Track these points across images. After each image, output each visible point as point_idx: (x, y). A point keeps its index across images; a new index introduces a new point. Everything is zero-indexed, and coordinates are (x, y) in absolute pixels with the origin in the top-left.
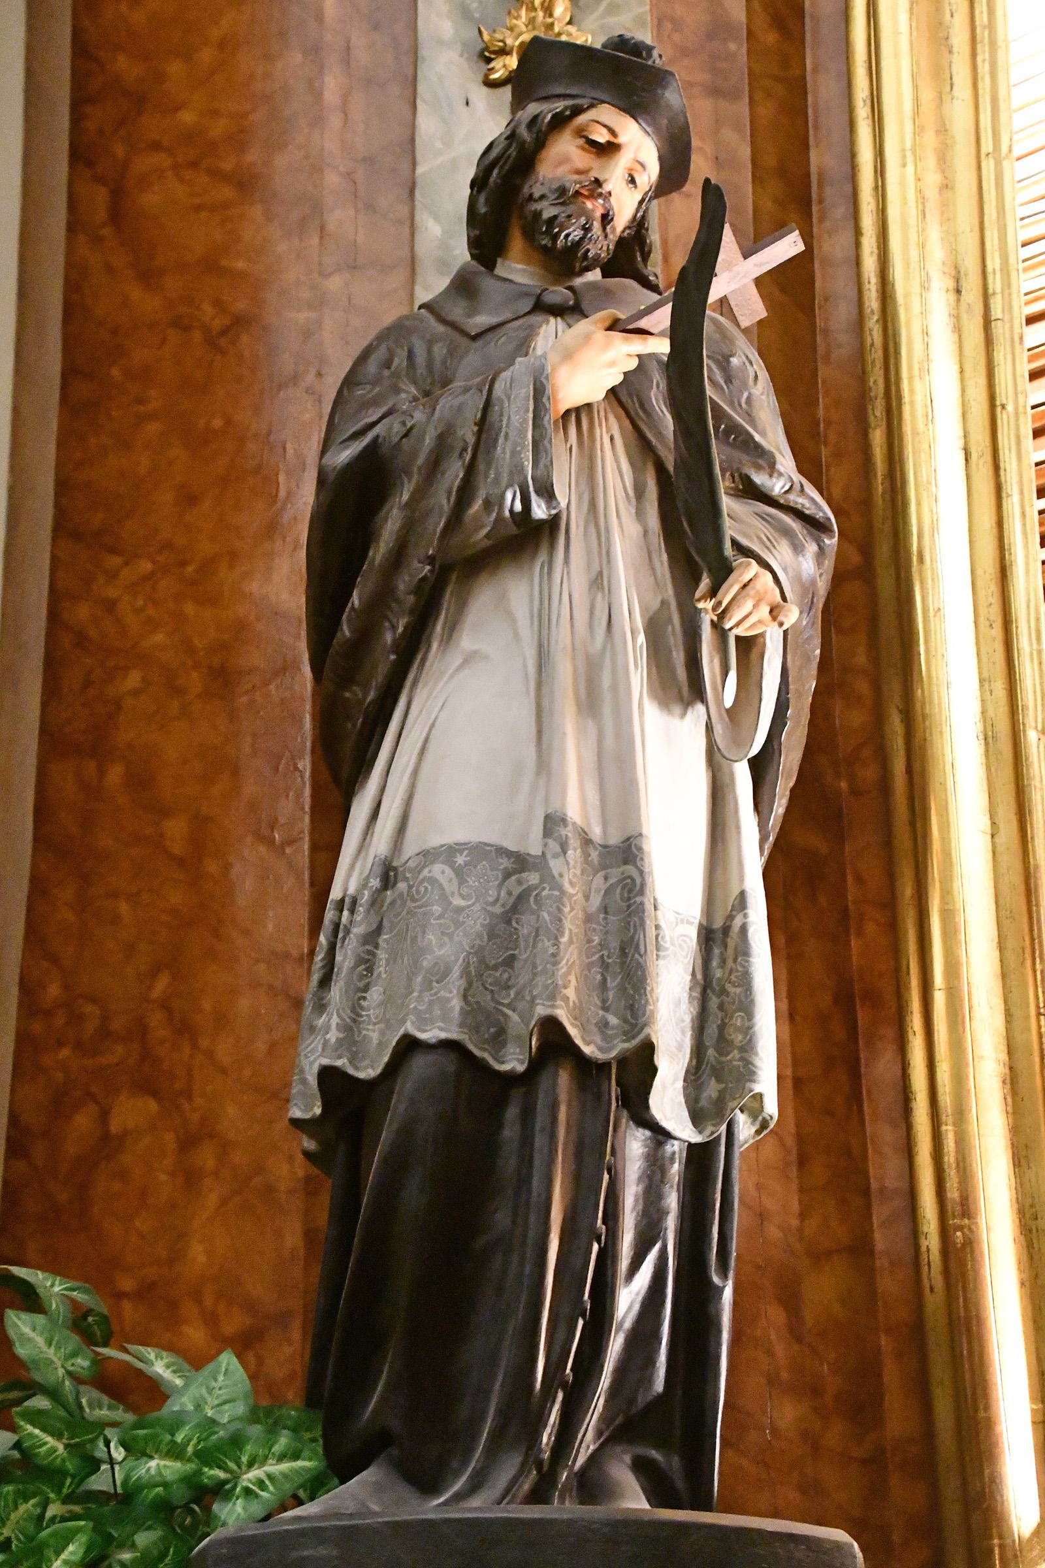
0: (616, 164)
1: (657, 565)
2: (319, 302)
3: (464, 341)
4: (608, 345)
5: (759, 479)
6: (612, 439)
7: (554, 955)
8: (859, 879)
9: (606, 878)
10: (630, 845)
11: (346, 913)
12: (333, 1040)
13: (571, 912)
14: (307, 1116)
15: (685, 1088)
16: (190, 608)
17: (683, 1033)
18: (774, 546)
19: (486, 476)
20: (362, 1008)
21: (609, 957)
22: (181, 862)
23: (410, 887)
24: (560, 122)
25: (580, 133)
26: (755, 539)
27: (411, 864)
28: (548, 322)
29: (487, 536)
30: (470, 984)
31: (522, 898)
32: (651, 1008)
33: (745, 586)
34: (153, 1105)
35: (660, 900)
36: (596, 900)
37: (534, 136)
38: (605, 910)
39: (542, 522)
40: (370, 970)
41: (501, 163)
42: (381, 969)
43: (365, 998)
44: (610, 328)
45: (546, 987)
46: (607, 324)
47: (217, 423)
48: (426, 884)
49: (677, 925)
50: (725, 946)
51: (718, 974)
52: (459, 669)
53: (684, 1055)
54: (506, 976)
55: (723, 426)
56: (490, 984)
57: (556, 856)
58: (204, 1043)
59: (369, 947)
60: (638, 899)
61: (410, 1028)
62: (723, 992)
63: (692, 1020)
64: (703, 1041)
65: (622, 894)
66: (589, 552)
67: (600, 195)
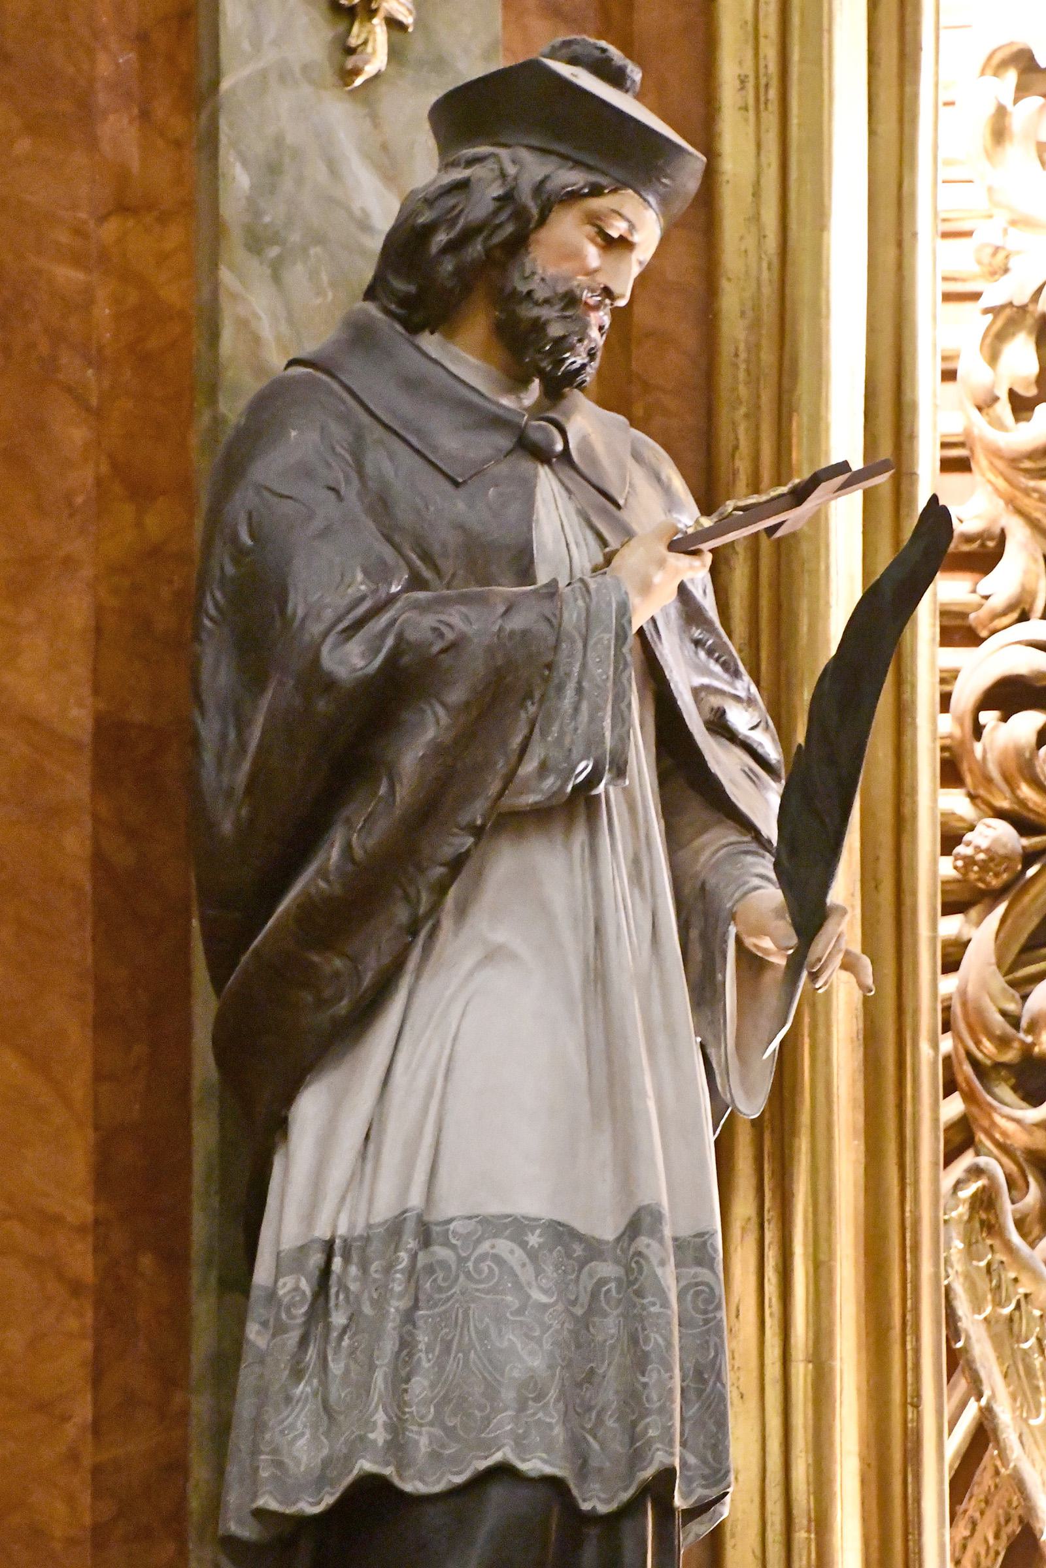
24: (573, 197)
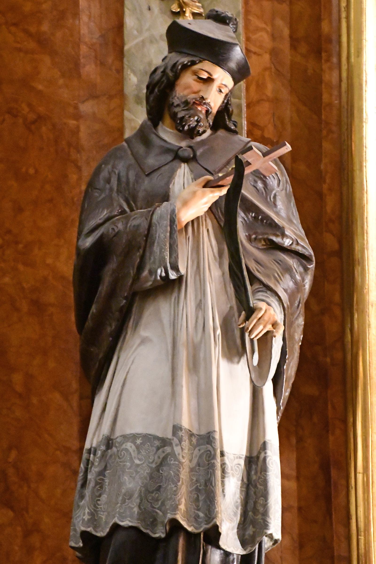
0: (212, 90)
1: (229, 289)
2: (78, 116)
3: (143, 176)
4: (204, 195)
5: (277, 240)
6: (208, 230)
7: (175, 491)
8: (334, 408)
9: (199, 450)
10: (209, 436)
11: (92, 455)
12: (86, 519)
13: (183, 470)
14: (77, 546)
15: (238, 532)
16: (21, 267)
17: (237, 508)
18: (281, 280)
19: (150, 259)
20: (98, 505)
21: (200, 486)
22: (20, 396)
23: (118, 451)
24: (185, 67)
25: (195, 73)
26: (273, 278)
27: (118, 440)
28: (181, 167)
29: (152, 285)
30: (141, 500)
31: (165, 459)
32: (217, 510)
33: (260, 318)
34: (11, 514)
35: (226, 449)
36: (195, 461)
37: (173, 74)
38: (199, 465)
39: (174, 280)
40: (101, 487)
41: (159, 85)
42: (107, 487)
43: (99, 500)
44: (204, 187)
45: (171, 505)
46: (203, 184)
47: (31, 171)
48: (124, 451)
49: (234, 460)
50: (257, 465)
51: (254, 477)
52: (139, 345)
53: (237, 519)
54: (157, 495)
55: (260, 217)
56: (150, 500)
57: (177, 445)
58: (33, 486)
59: (101, 477)
60: (212, 461)
61: (116, 520)
62: (256, 486)
63: (241, 502)
64: (247, 508)
65: (206, 458)
66: (196, 290)
67: (205, 104)
